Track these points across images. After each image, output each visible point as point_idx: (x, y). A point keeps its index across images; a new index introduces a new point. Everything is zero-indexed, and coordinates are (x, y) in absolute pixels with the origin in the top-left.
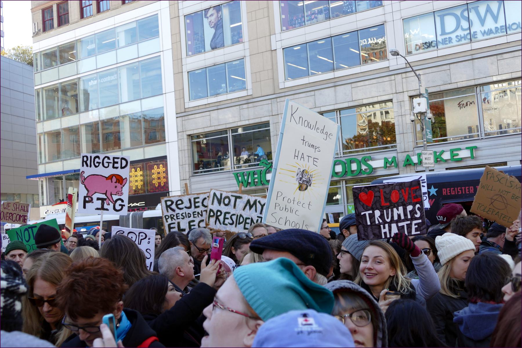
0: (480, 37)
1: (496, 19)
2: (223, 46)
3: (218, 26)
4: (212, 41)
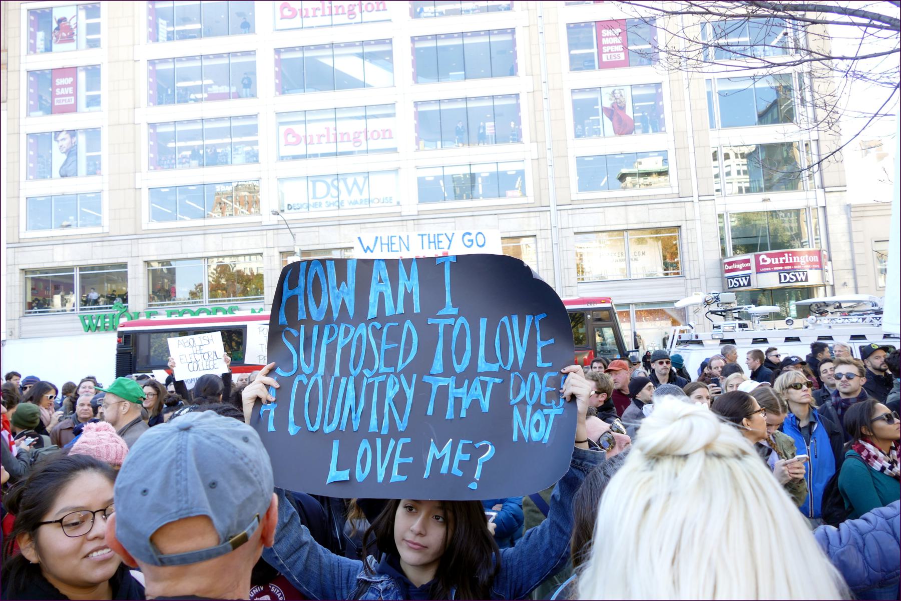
0: (346, 205)
1: (361, 191)
2: (75, 174)
3: (71, 152)
4: (62, 167)
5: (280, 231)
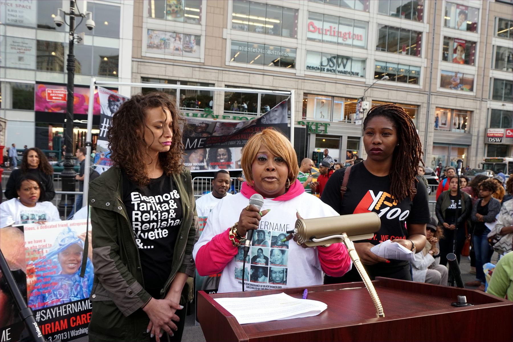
1: (344, 67)
5: (305, 81)
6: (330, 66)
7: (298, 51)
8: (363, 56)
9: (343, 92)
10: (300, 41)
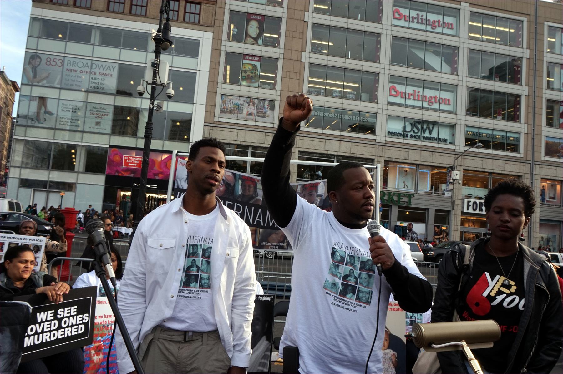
5: (387, 148)
6: (414, 132)
7: (379, 117)
8: (452, 121)
9: (430, 160)
10: (380, 106)
